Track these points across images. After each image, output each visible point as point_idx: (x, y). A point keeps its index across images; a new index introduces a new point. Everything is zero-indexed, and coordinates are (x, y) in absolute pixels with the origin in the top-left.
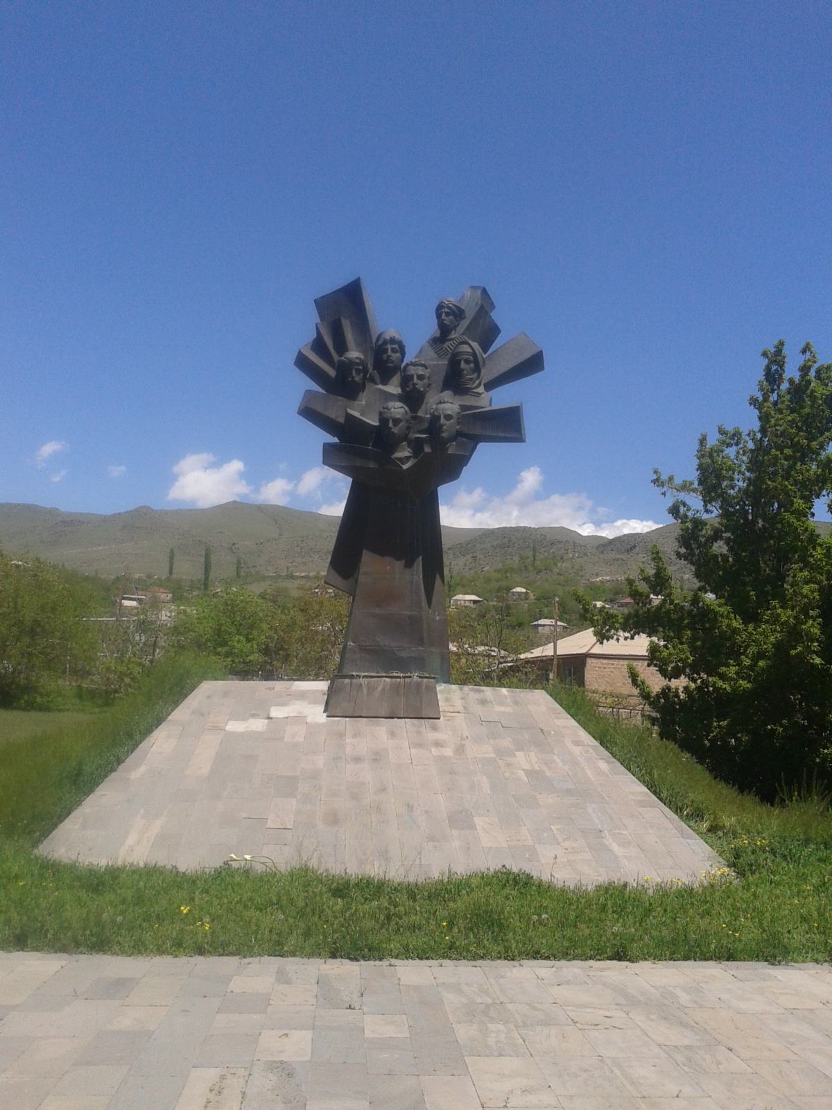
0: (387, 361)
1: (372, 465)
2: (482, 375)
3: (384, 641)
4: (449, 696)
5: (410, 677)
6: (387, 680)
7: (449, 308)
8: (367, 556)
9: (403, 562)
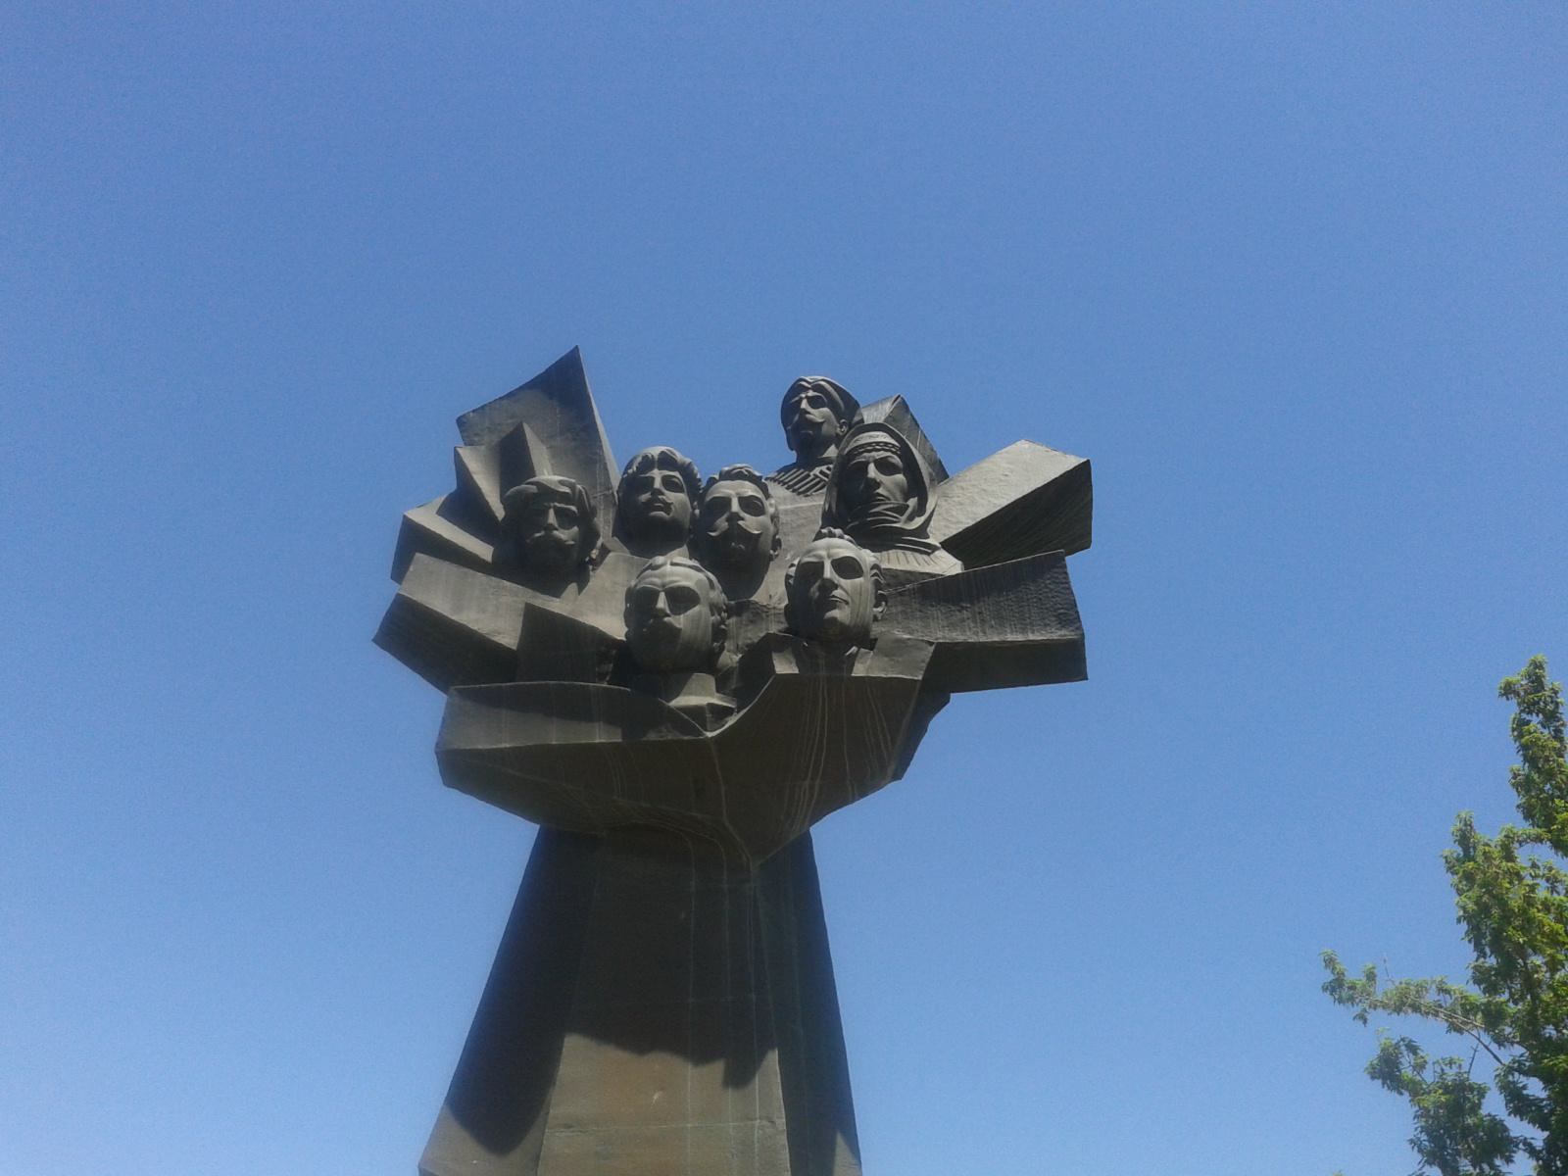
1: (600, 735)
7: (817, 388)
9: (716, 1069)
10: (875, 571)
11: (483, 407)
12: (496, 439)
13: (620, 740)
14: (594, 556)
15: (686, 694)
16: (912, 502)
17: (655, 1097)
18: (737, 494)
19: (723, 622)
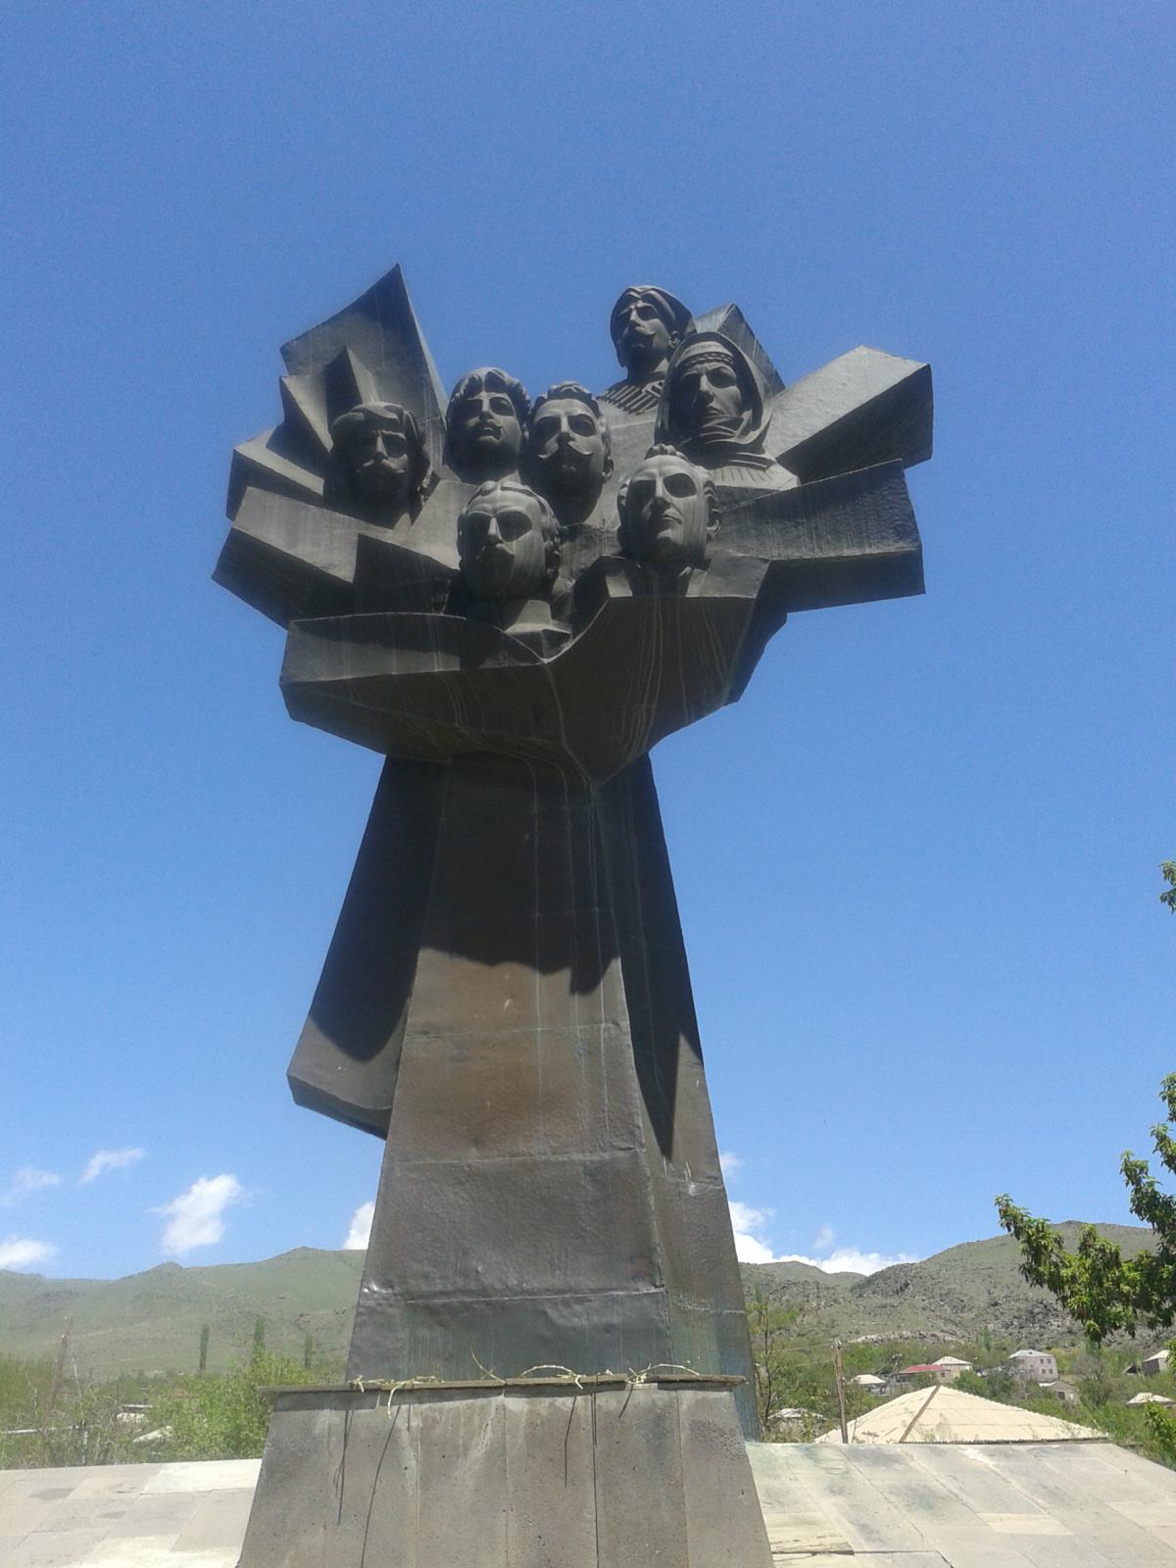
0: (479, 430)
1: (439, 664)
2: (765, 418)
3: (502, 1271)
4: (776, 1483)
5: (619, 1385)
6: (516, 1404)
7: (647, 297)
8: (434, 974)
9: (564, 977)
10: (707, 489)
11: (304, 335)
12: (320, 367)
13: (458, 669)
14: (425, 486)
15: (523, 621)
16: (747, 415)
17: (507, 1004)
18: (567, 413)
19: (556, 547)
